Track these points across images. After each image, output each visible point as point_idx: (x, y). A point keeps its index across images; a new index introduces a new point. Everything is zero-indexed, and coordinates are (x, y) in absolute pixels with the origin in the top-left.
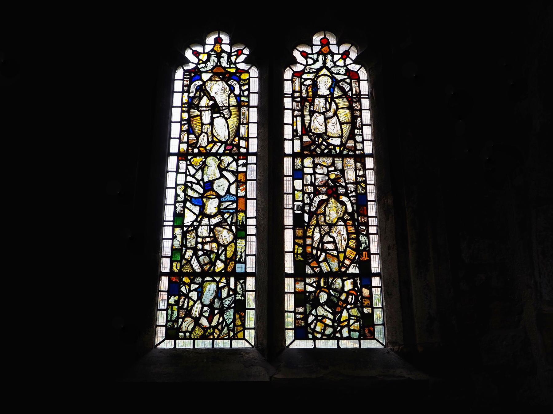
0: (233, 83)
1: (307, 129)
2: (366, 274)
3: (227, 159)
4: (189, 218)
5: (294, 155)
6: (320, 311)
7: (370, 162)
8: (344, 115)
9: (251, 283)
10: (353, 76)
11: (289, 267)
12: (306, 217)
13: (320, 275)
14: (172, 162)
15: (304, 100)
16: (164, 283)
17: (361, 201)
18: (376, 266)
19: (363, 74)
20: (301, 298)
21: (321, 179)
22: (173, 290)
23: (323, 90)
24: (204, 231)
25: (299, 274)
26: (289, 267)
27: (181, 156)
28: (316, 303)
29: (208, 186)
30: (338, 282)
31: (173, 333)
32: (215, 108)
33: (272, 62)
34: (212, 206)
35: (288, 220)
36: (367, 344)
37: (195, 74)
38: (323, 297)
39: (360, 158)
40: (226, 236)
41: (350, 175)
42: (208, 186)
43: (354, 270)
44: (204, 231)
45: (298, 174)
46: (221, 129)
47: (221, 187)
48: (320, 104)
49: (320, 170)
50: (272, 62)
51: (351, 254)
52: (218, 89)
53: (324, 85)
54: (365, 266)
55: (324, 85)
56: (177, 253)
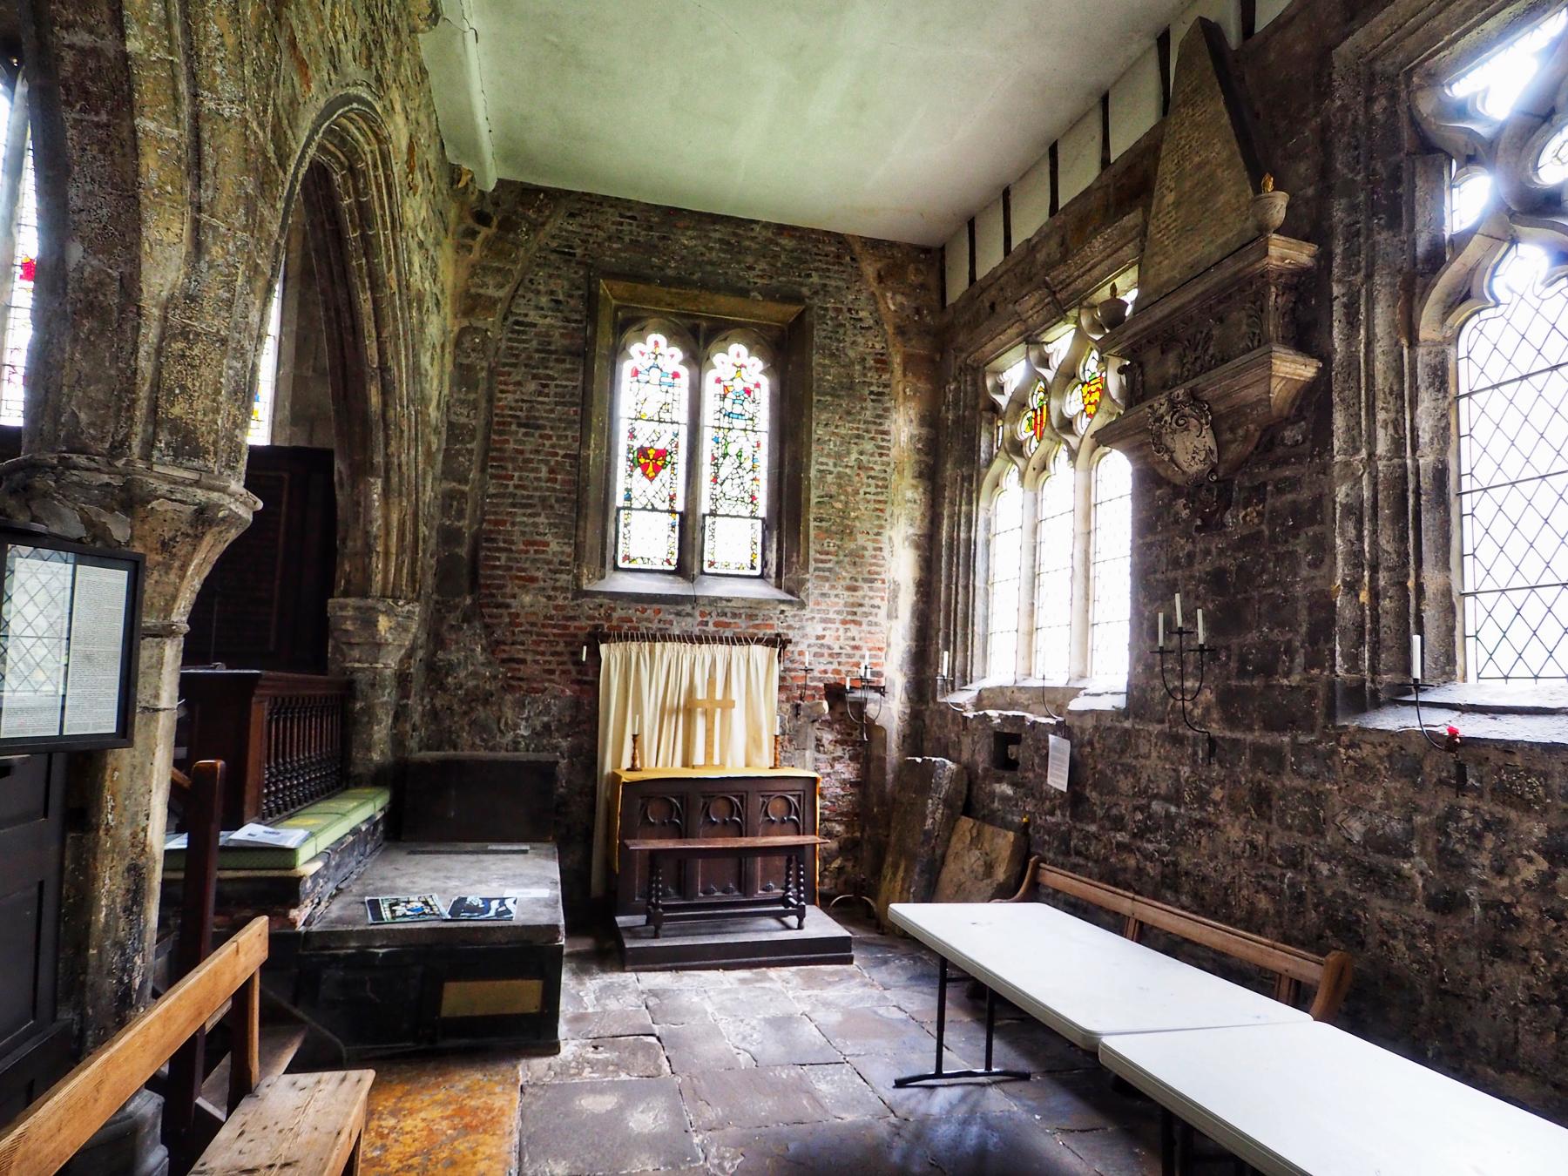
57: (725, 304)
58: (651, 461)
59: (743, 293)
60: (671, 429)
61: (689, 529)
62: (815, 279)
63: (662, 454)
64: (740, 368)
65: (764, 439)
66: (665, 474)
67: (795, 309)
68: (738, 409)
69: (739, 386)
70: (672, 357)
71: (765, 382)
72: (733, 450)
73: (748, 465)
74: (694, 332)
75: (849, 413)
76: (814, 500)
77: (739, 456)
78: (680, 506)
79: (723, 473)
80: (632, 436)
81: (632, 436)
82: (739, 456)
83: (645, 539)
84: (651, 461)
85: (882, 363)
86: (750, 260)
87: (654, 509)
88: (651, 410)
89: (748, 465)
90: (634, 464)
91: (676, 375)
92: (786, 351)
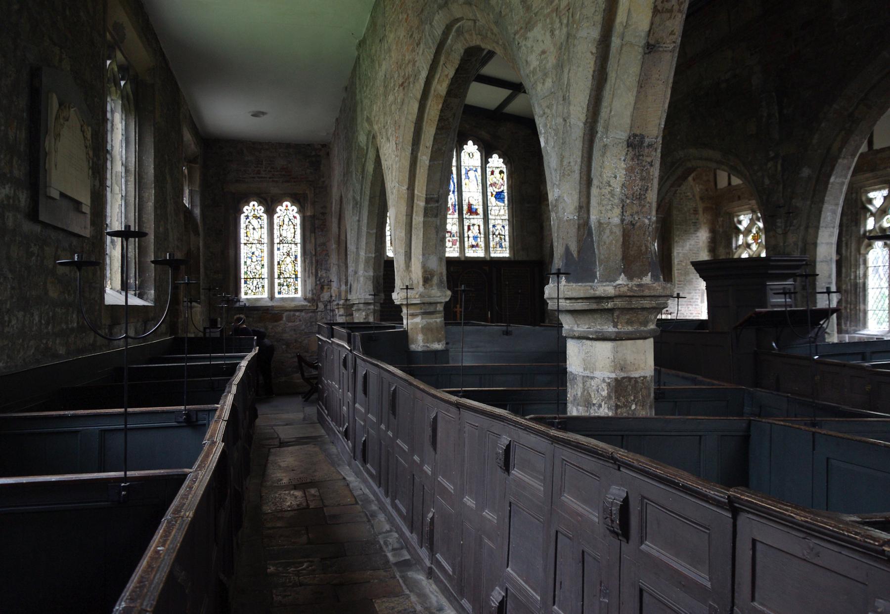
2: (296, 278)
3: (258, 245)
4: (248, 263)
7: (299, 245)
8: (293, 231)
9: (266, 280)
10: (295, 217)
11: (276, 276)
14: (242, 246)
16: (243, 281)
17: (296, 257)
18: (299, 275)
19: (298, 216)
20: (280, 284)
21: (285, 251)
22: (246, 282)
23: (286, 222)
24: (253, 266)
25: (279, 278)
26: (276, 276)
27: (245, 244)
29: (253, 253)
31: (246, 294)
32: (254, 229)
33: (270, 212)
34: (254, 259)
35: (276, 263)
36: (296, 296)
37: (247, 217)
39: (296, 244)
40: (259, 267)
41: (293, 250)
42: (253, 253)
44: (253, 266)
45: (279, 249)
46: (256, 235)
47: (257, 253)
48: (285, 227)
49: (285, 248)
50: (270, 212)
52: (255, 222)
53: (286, 220)
54: (296, 275)
55: (286, 220)
56: (246, 273)
85: (696, 211)
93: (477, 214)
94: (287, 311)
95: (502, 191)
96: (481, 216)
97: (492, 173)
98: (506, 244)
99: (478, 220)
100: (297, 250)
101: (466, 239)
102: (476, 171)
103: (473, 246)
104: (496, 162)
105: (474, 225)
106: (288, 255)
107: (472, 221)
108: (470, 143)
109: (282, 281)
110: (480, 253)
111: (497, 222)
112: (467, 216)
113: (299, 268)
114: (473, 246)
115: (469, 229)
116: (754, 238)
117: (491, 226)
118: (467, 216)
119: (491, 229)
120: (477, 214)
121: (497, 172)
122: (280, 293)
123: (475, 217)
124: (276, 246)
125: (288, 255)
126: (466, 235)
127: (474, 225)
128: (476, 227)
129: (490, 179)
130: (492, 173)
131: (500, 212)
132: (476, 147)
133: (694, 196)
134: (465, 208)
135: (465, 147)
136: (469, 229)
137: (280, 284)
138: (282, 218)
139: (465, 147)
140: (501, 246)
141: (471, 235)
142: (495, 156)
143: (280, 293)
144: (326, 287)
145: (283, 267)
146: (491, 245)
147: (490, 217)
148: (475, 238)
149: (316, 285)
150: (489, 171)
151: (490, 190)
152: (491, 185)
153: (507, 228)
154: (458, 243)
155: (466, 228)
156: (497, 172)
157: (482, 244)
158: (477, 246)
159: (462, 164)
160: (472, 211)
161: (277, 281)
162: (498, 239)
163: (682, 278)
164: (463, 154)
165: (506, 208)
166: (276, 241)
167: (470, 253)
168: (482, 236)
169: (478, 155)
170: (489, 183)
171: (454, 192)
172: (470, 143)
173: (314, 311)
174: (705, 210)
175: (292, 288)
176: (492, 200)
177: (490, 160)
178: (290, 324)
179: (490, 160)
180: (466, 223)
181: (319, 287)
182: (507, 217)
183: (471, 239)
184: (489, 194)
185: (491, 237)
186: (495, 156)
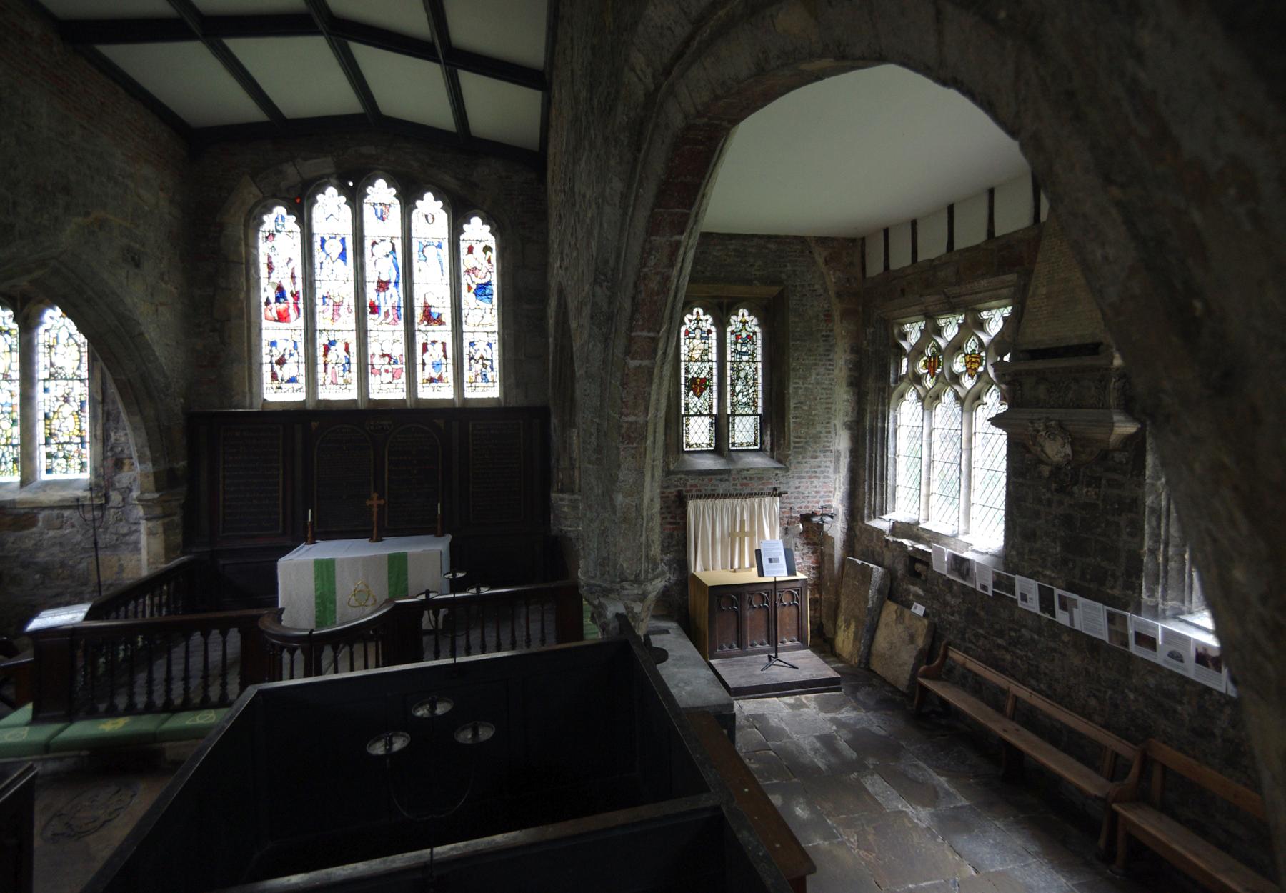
0: (6, 336)
1: (52, 365)
2: (83, 443)
5: (45, 380)
6: (59, 461)
12: (51, 415)
13: (59, 444)
15: (50, 347)
18: (88, 439)
20: (49, 456)
25: (47, 443)
28: (56, 457)
30: (68, 447)
38: (61, 454)
43: (78, 440)
45: (46, 390)
48: (60, 349)
49: (58, 388)
51: (77, 433)
57: (738, 290)
58: (698, 386)
59: (749, 282)
60: (708, 365)
61: (721, 426)
62: (789, 268)
63: (704, 380)
64: (744, 321)
65: (760, 366)
66: (706, 393)
67: (775, 290)
68: (744, 349)
69: (744, 334)
70: (707, 322)
71: (757, 329)
72: (742, 374)
73: (751, 383)
74: (720, 306)
75: (810, 350)
76: (792, 406)
77: (746, 377)
78: (715, 411)
79: (738, 389)
80: (687, 372)
81: (687, 372)
82: (746, 377)
83: (699, 432)
84: (698, 386)
85: (828, 316)
86: (752, 261)
87: (701, 415)
88: (696, 355)
89: (751, 383)
90: (689, 388)
91: (709, 332)
92: (770, 316)
93: (439, 321)
94: (44, 508)
95: (489, 283)
96: (448, 326)
97: (470, 250)
98: (494, 375)
99: (443, 334)
100: (80, 391)
101: (419, 368)
102: (439, 246)
103: (432, 380)
104: (477, 231)
105: (434, 342)
106: (66, 400)
107: (431, 337)
108: (429, 196)
109: (53, 449)
110: (445, 392)
111: (477, 337)
112: (422, 327)
113: (86, 426)
114: (432, 380)
115: (425, 349)
116: (927, 365)
117: (466, 344)
118: (422, 327)
119: (466, 350)
120: (439, 321)
121: (478, 248)
122: (49, 471)
123: (436, 327)
124: (39, 387)
125: (66, 400)
126: (419, 360)
127: (434, 342)
128: (439, 347)
129: (467, 261)
130: (470, 250)
131: (483, 323)
132: (440, 204)
133: (826, 290)
134: (419, 313)
135: (418, 203)
136: (425, 349)
137: (49, 456)
138: (53, 333)
139: (418, 203)
140: (485, 378)
141: (428, 360)
142: (476, 221)
143: (49, 471)
144: (126, 461)
145: (55, 424)
146: (466, 378)
147: (465, 328)
148: (436, 365)
149: (105, 458)
150: (464, 247)
151: (465, 280)
152: (468, 271)
153: (496, 347)
154: (403, 376)
155: (419, 348)
156: (478, 248)
157: (449, 375)
158: (440, 379)
159: (414, 234)
160: (429, 317)
161: (41, 452)
162: (478, 367)
163: (802, 432)
164: (415, 215)
165: (495, 312)
166: (41, 372)
167: (426, 392)
168: (450, 361)
169: (442, 219)
170: (463, 269)
171: (396, 284)
172: (429, 196)
173: (101, 507)
174: (845, 314)
175: (75, 462)
176: (468, 299)
177: (465, 227)
178: (51, 533)
179: (465, 227)
180: (420, 339)
181: (110, 463)
182: (496, 328)
183: (428, 368)
184: (464, 288)
185: (466, 362)
186: (476, 221)
